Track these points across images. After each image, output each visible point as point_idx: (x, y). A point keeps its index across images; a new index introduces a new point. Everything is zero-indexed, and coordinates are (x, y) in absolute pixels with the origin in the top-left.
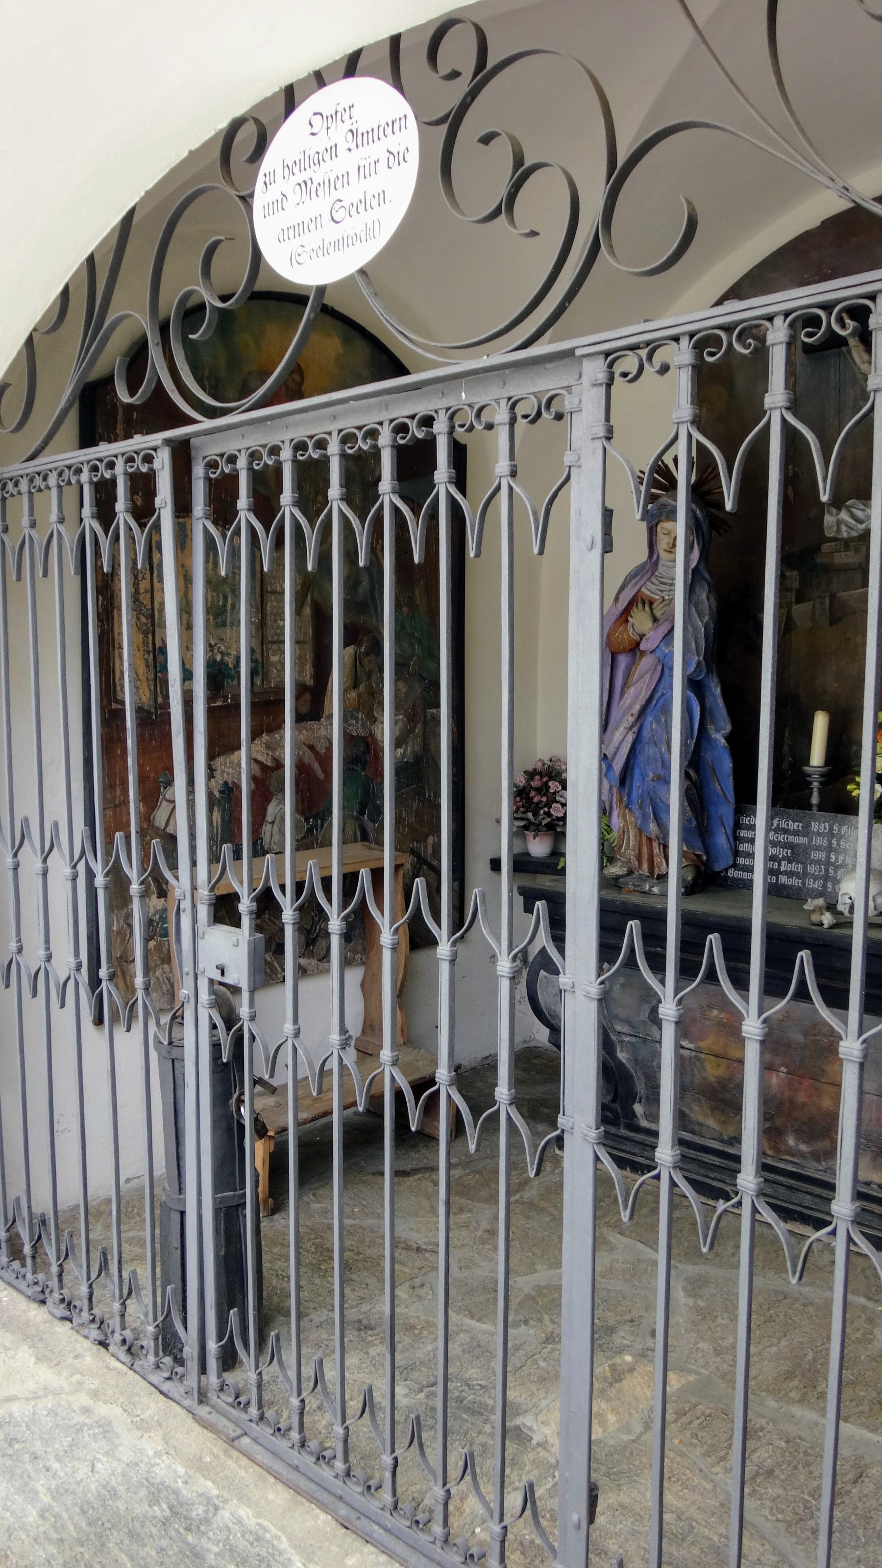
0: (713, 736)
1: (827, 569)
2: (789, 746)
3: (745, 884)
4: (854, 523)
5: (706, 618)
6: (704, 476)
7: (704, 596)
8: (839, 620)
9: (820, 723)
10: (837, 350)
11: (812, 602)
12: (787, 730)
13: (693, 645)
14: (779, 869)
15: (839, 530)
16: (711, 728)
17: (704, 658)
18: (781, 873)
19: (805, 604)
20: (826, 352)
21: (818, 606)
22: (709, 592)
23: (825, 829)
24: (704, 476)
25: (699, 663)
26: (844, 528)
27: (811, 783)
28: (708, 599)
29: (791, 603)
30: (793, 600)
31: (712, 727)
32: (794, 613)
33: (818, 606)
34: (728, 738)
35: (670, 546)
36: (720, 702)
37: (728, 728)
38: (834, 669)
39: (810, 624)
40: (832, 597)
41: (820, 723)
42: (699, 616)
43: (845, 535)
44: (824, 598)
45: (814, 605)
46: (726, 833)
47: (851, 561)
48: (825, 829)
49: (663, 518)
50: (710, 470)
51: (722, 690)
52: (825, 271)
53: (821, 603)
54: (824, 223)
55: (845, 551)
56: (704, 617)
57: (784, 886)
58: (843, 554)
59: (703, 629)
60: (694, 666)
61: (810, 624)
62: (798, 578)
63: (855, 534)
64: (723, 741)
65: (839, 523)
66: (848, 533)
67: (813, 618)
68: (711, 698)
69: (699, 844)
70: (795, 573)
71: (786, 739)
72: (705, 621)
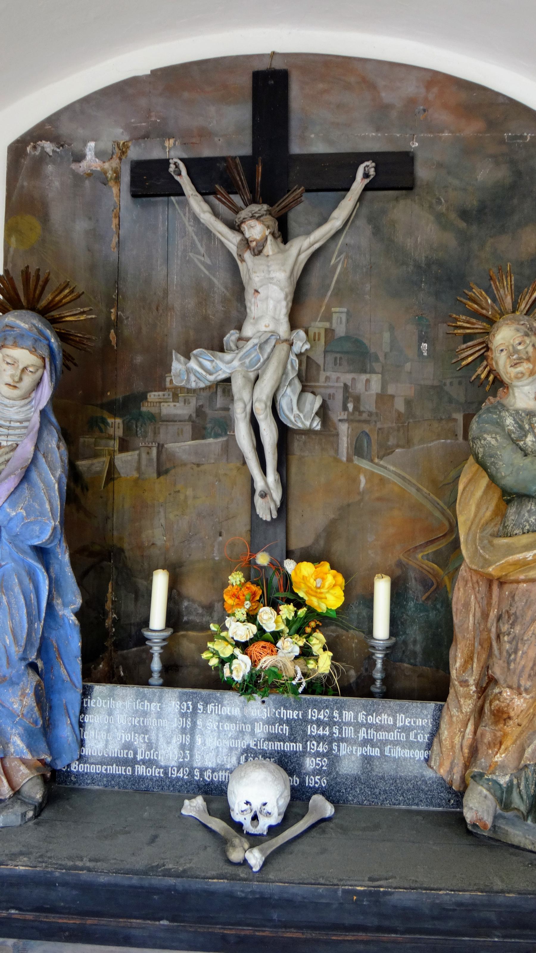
0: (61, 613)
1: (153, 418)
2: (113, 602)
3: (93, 779)
4: (204, 373)
5: (59, 472)
6: (58, 299)
7: (53, 443)
8: (167, 472)
9: (160, 582)
10: (165, 199)
11: (137, 452)
12: (110, 583)
13: (47, 506)
14: (135, 757)
15: (188, 380)
16: (58, 602)
17: (61, 522)
18: (138, 763)
19: (130, 453)
20: (153, 199)
21: (144, 456)
22: (59, 440)
23: (188, 708)
24: (58, 299)
25: (55, 529)
26: (193, 378)
27: (151, 648)
28: (59, 448)
29: (114, 451)
30: (117, 448)
31: (59, 601)
32: (118, 463)
33: (144, 456)
34: (79, 614)
35: (17, 379)
36: (69, 571)
37: (79, 602)
38: (163, 521)
39: (136, 475)
40: (160, 448)
41: (160, 582)
42: (51, 469)
43: (193, 385)
44: (150, 448)
45: (139, 455)
46: (71, 723)
47: (179, 412)
48: (188, 708)
49: (10, 342)
50: (67, 291)
51: (71, 556)
52: (153, 119)
53: (148, 453)
54: (154, 72)
55: (173, 401)
56: (56, 470)
57: (142, 778)
58: (172, 404)
59: (56, 486)
60: (49, 534)
61: (136, 475)
62: (121, 426)
63: (202, 385)
64: (73, 618)
65: (189, 371)
66: (197, 384)
67: (138, 469)
68: (57, 567)
69: (43, 745)
70: (119, 421)
71: (109, 595)
72: (57, 475)
